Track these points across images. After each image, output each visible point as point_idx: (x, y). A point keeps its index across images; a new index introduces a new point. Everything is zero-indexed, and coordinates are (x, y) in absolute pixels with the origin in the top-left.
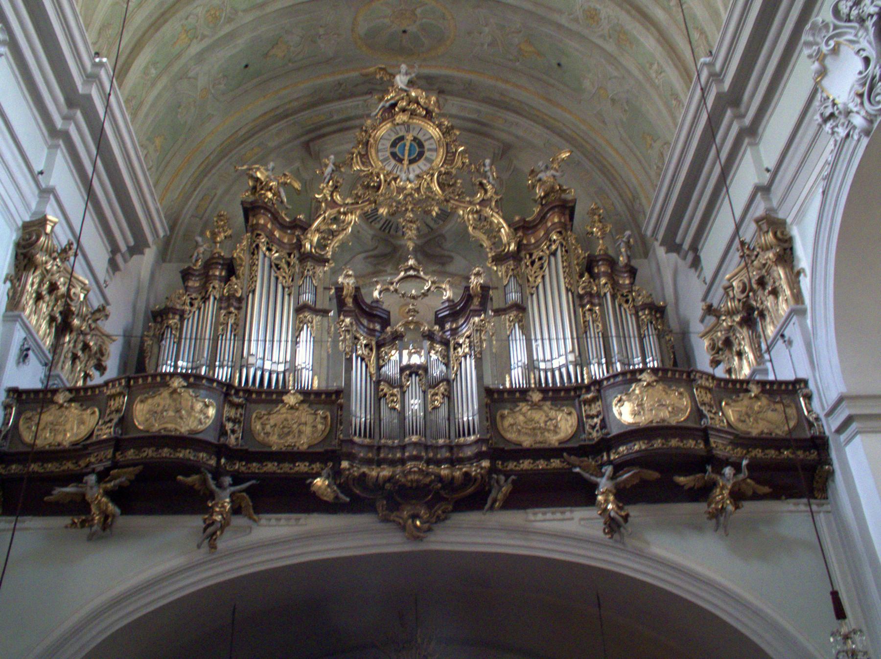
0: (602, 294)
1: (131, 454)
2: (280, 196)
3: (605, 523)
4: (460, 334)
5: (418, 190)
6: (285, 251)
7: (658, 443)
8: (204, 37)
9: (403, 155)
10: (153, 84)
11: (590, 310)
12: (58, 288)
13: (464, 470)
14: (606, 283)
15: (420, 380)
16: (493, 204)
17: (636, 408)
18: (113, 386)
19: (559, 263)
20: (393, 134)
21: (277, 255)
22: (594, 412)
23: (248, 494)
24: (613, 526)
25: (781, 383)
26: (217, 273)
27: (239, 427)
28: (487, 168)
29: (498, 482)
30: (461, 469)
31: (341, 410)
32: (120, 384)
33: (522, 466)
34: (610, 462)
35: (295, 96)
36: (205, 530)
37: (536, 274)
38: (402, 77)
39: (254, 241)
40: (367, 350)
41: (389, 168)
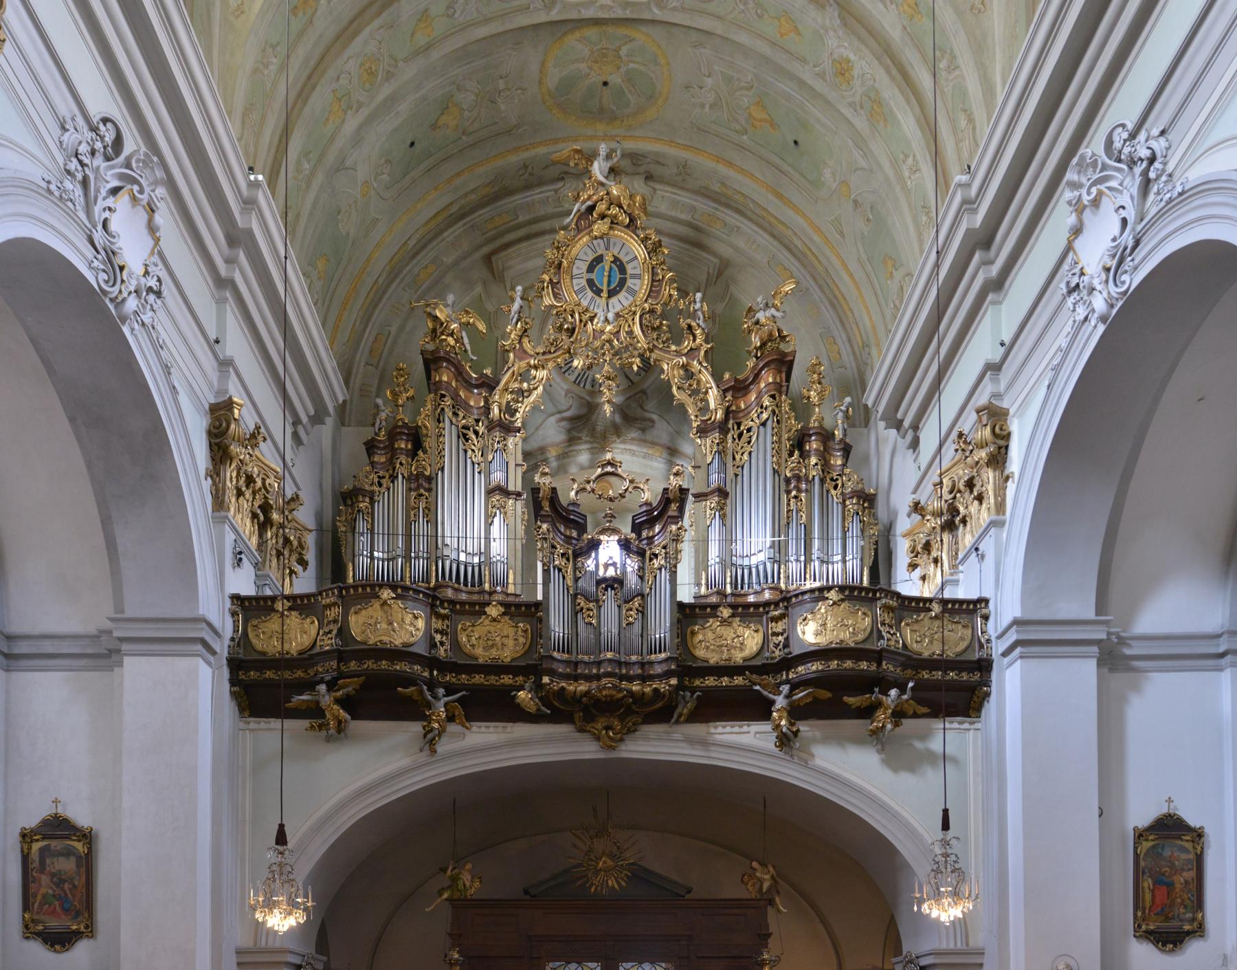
12: (255, 482)
13: (654, 686)
15: (616, 594)
18: (327, 595)
20: (589, 252)
29: (684, 697)
30: (651, 685)
34: (788, 681)
35: (472, 186)
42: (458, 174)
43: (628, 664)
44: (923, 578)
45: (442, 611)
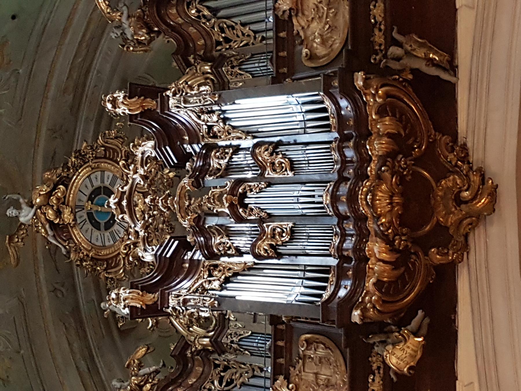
38: (22, 214)
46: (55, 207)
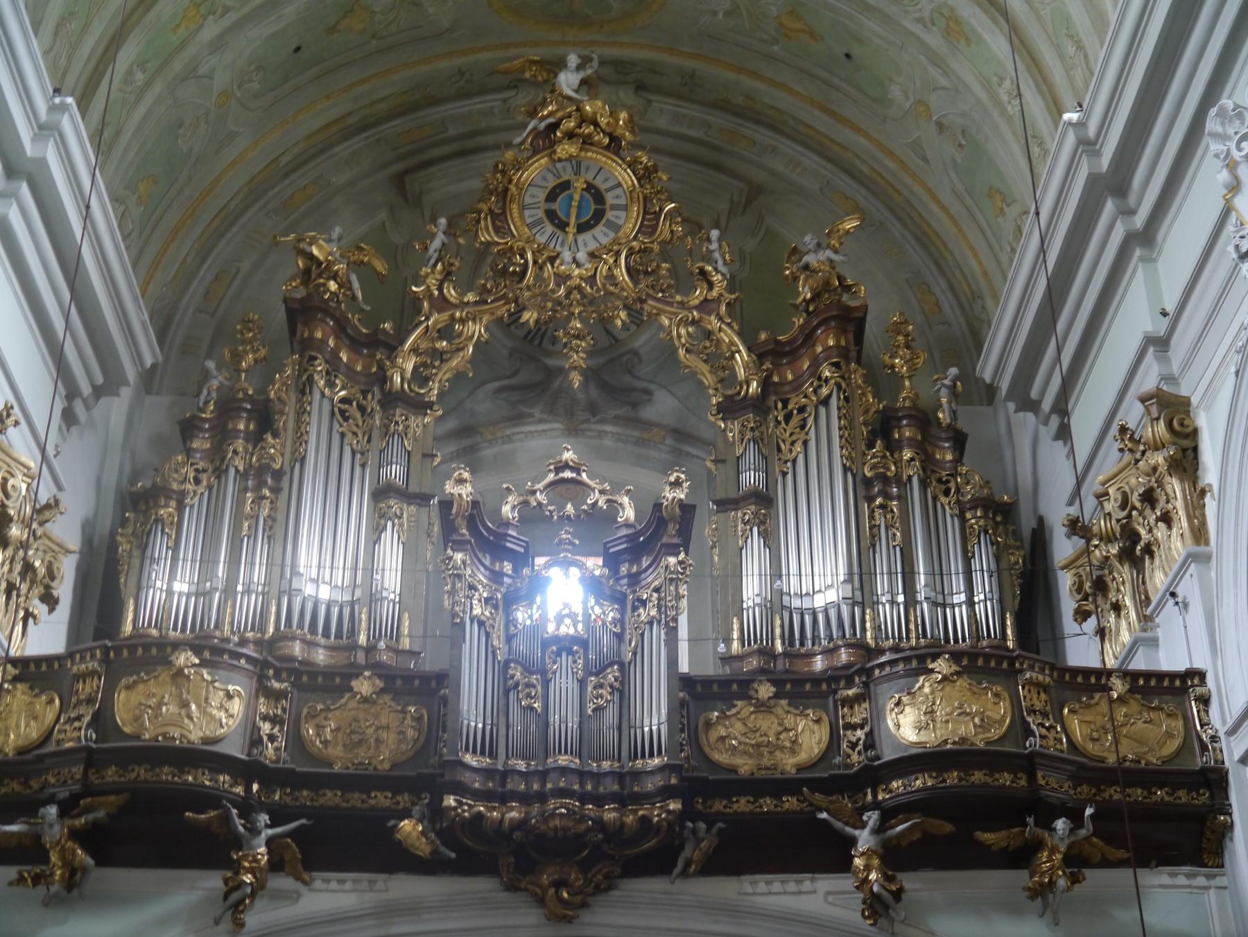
0: (905, 477)
1: (111, 774)
2: (351, 289)
3: (864, 903)
4: (643, 583)
5: (591, 280)
6: (357, 387)
7: (953, 778)
8: (227, 9)
9: (568, 216)
10: (140, 94)
11: (882, 506)
13: (641, 813)
14: (912, 459)
16: (723, 308)
17: (923, 718)
19: (831, 420)
20: (550, 177)
21: (343, 393)
22: (856, 720)
23: (293, 840)
24: (877, 907)
25: (1160, 676)
26: (242, 427)
27: (281, 730)
28: (714, 246)
29: (694, 831)
30: (635, 812)
31: (445, 706)
32: (93, 657)
33: (735, 806)
34: (876, 805)
36: (226, 896)
37: (794, 438)
39: (306, 370)
40: (489, 608)
41: (542, 239)
42: (363, 81)
43: (598, 777)
44: (1101, 632)
45: (276, 685)
46: (577, 130)
